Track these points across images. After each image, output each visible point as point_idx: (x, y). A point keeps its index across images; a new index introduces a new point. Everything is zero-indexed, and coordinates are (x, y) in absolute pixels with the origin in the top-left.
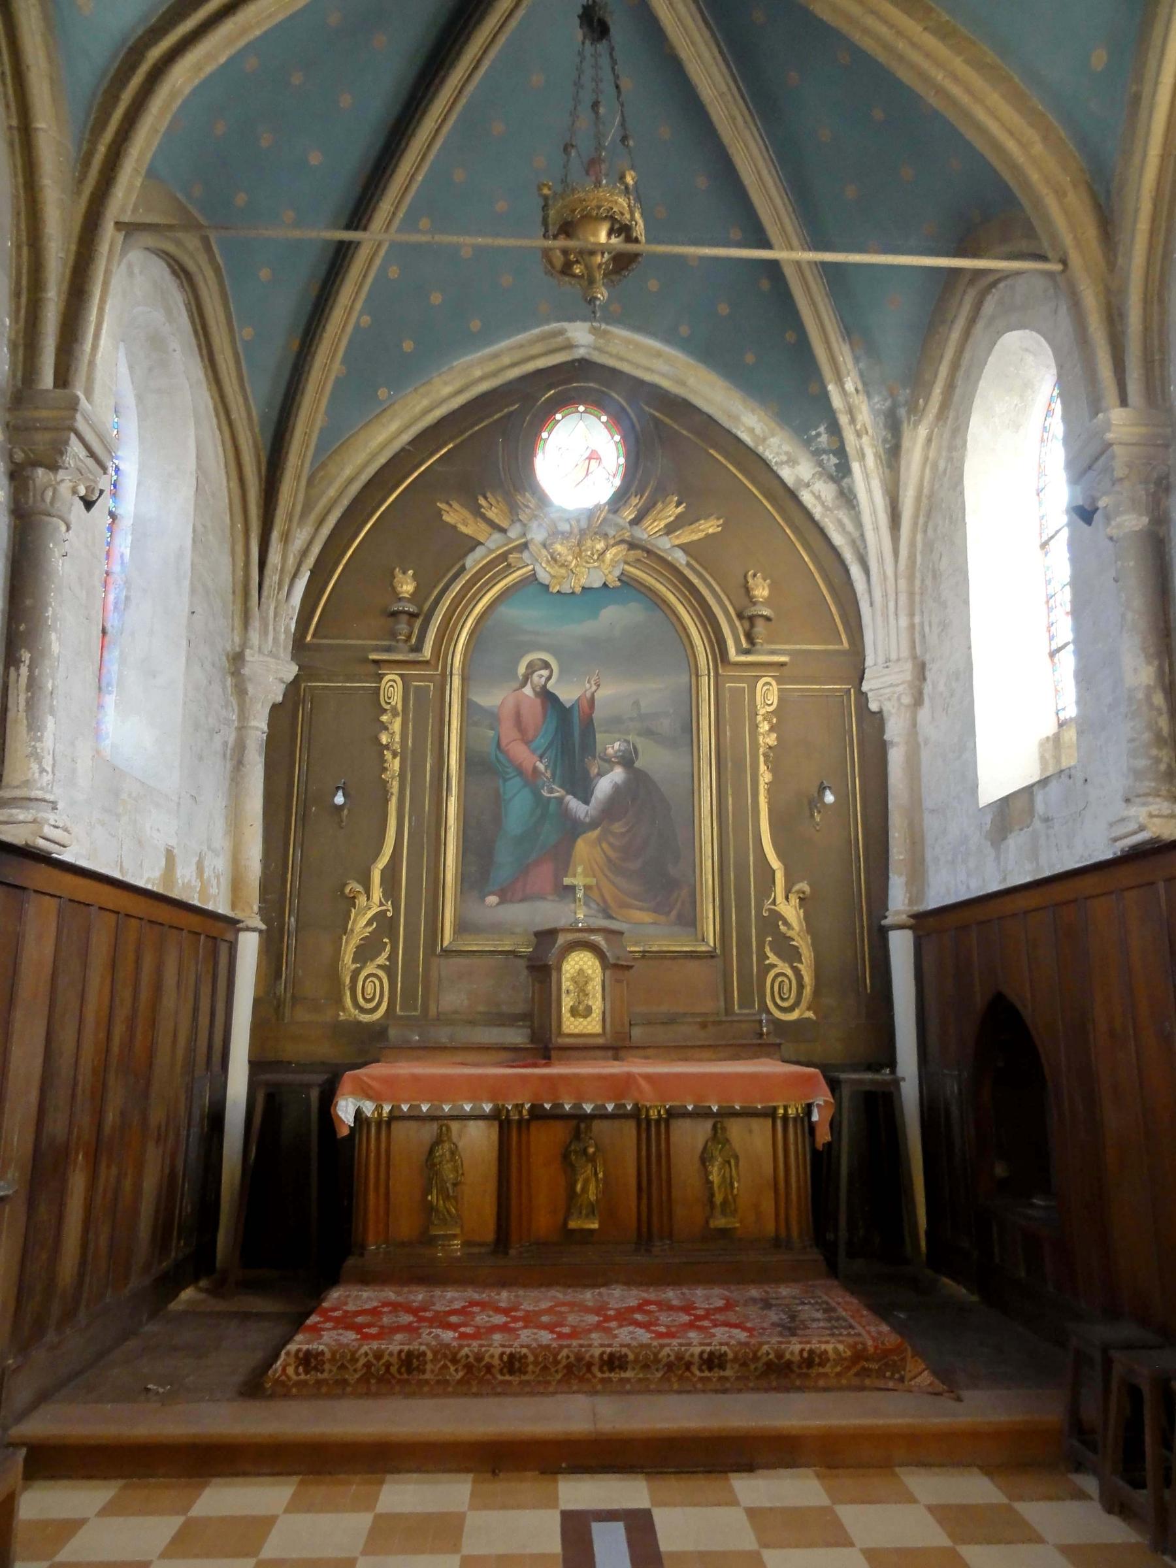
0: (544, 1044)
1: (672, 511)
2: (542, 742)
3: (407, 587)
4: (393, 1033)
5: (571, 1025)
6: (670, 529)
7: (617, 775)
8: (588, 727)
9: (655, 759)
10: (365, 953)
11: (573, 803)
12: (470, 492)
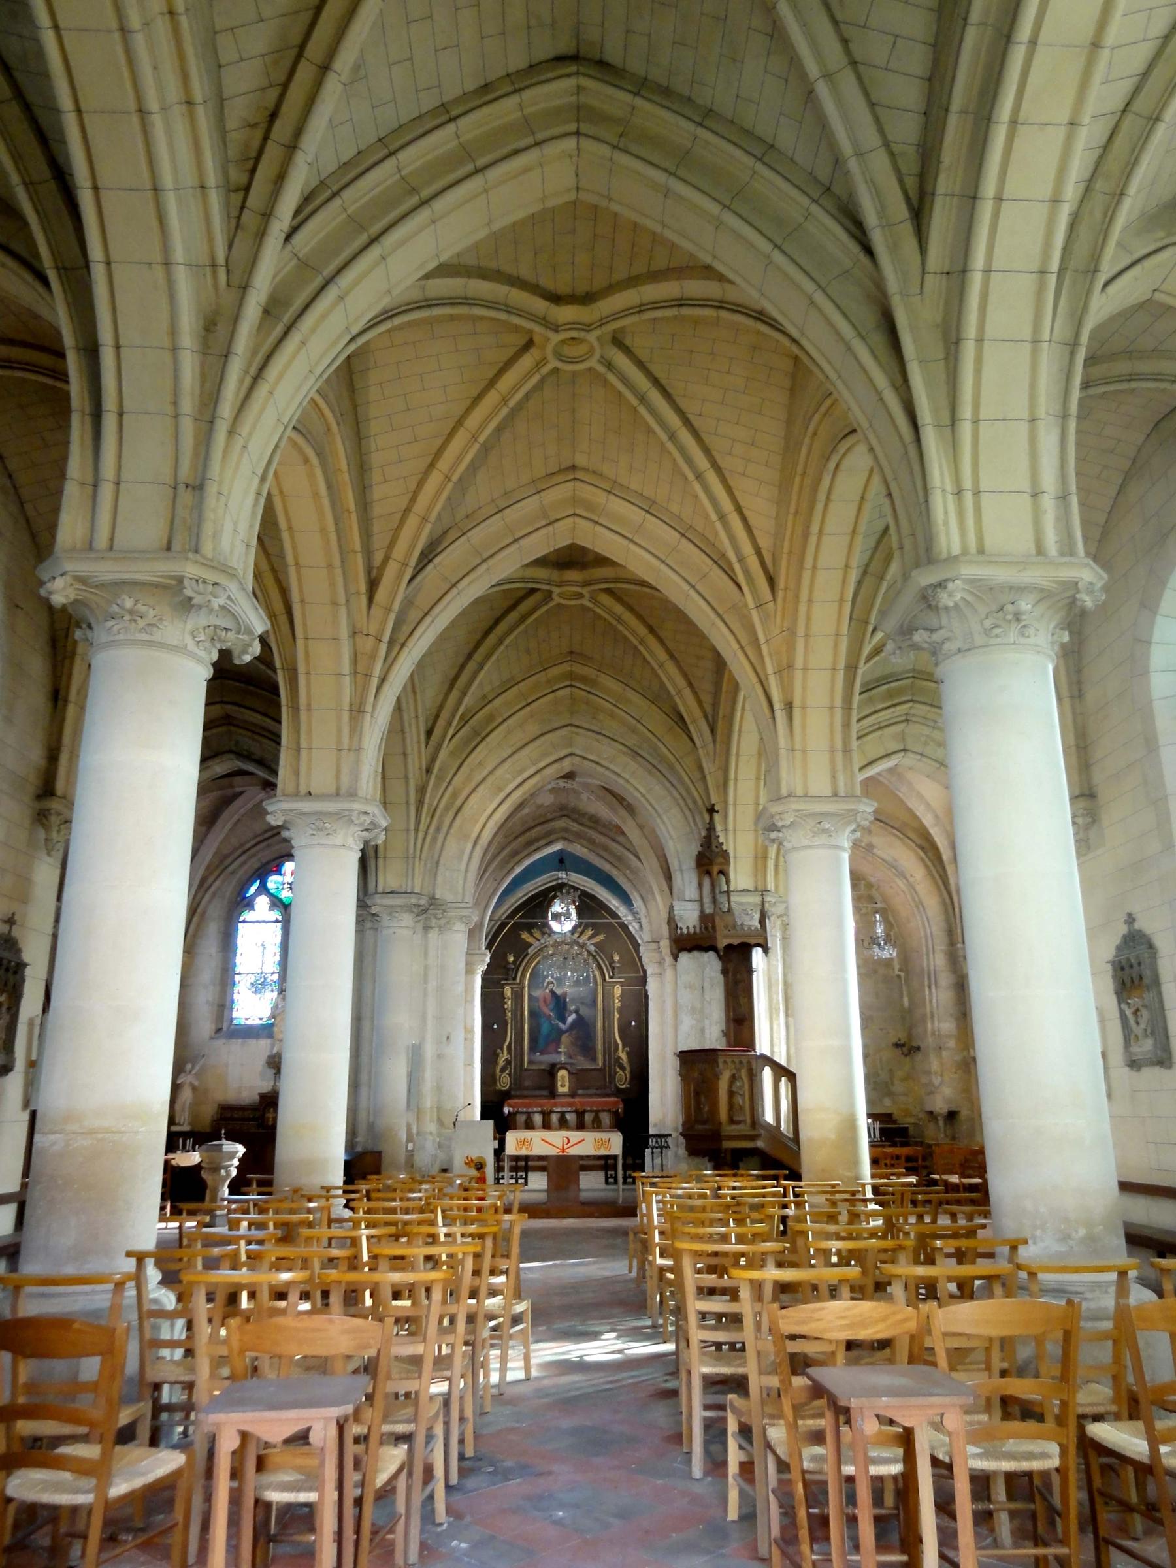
0: (553, 1094)
1: (590, 932)
2: (552, 1006)
3: (511, 959)
4: (513, 1093)
5: (560, 1089)
6: (589, 938)
7: (574, 1016)
8: (565, 1002)
9: (584, 1011)
10: (503, 1070)
11: (561, 1025)
12: (529, 928)
